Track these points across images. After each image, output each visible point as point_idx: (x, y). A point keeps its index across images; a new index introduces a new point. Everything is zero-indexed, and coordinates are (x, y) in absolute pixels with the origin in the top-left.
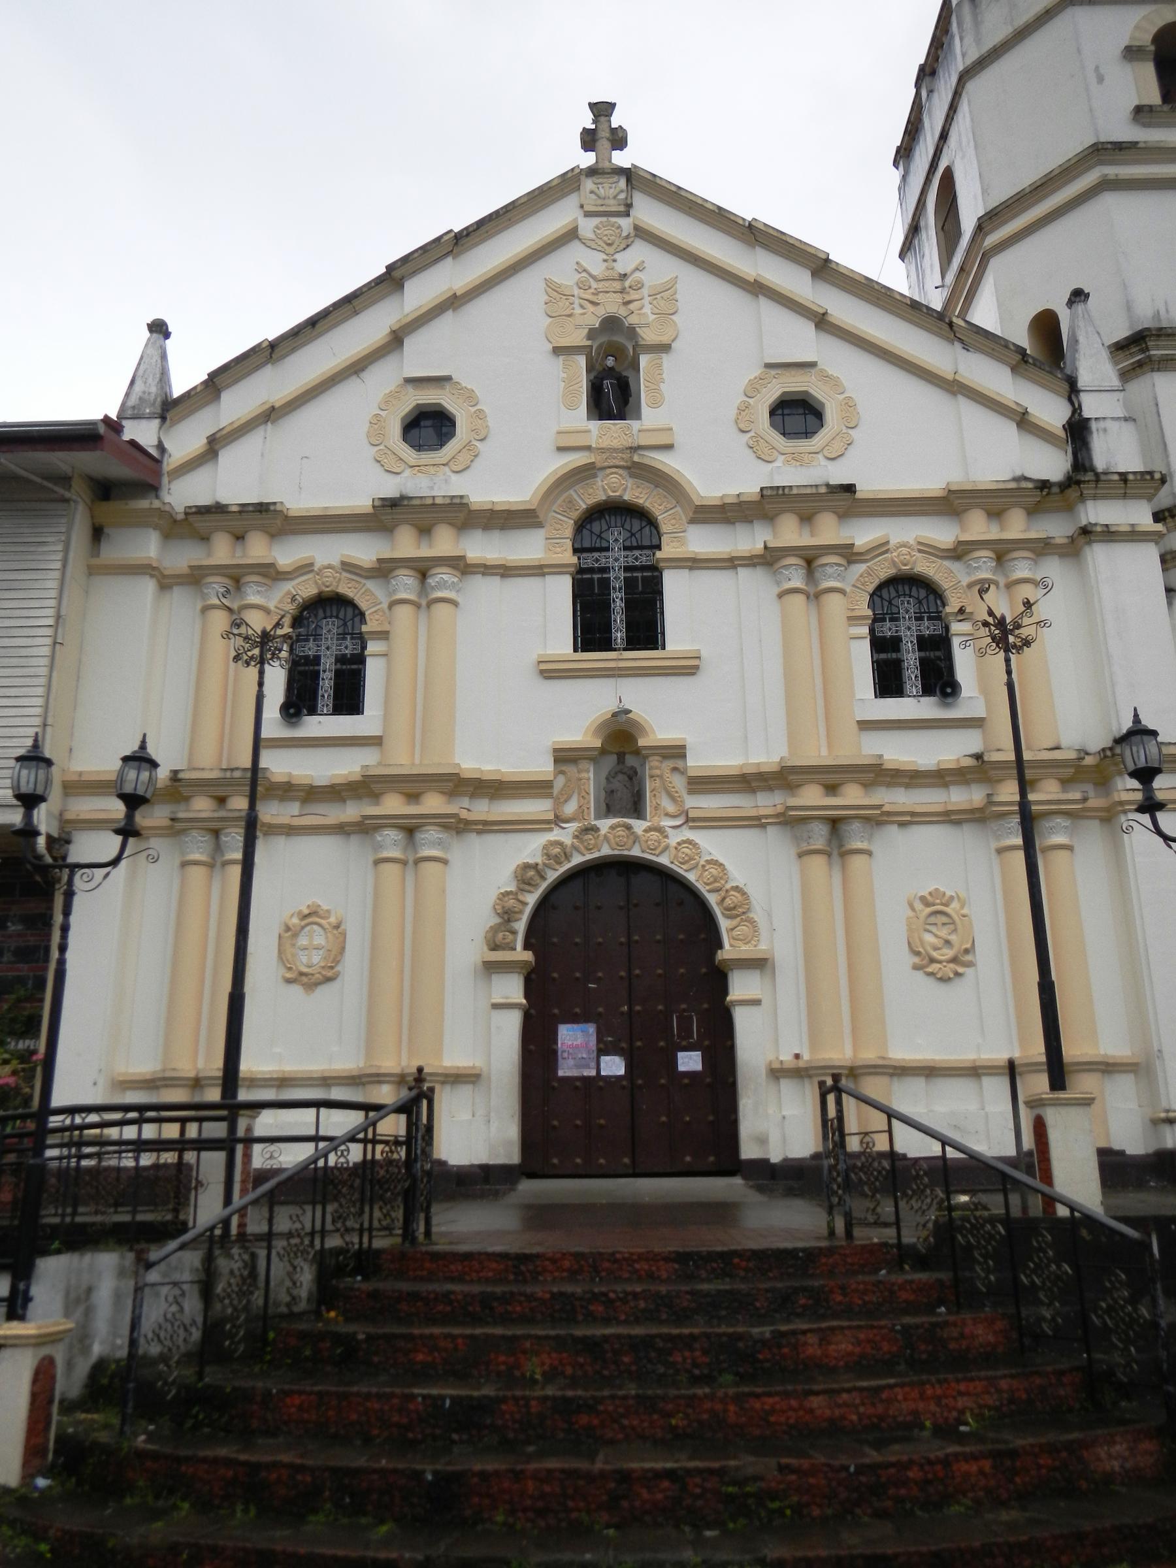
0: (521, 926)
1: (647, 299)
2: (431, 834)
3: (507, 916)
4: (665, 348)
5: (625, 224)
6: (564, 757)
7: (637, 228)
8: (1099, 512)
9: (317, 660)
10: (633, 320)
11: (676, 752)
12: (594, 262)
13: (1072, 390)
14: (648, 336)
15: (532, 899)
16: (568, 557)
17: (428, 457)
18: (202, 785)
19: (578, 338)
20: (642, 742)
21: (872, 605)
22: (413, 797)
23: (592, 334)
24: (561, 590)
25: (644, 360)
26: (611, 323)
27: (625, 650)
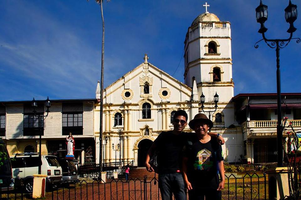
0: (137, 145)
1: (150, 79)
2: (129, 137)
3: (136, 145)
4: (152, 85)
5: (148, 70)
6: (142, 130)
7: (149, 71)
8: (193, 105)
9: (117, 119)
10: (149, 82)
11: (152, 129)
12: (145, 75)
13: (192, 91)
14: (150, 84)
15: (138, 143)
16: (142, 109)
17: (127, 98)
18: (108, 133)
19: (143, 84)
20: (149, 128)
21: (171, 114)
22: (127, 134)
23: (144, 84)
24: (141, 112)
25: (150, 86)
26: (146, 82)
27: (148, 118)
